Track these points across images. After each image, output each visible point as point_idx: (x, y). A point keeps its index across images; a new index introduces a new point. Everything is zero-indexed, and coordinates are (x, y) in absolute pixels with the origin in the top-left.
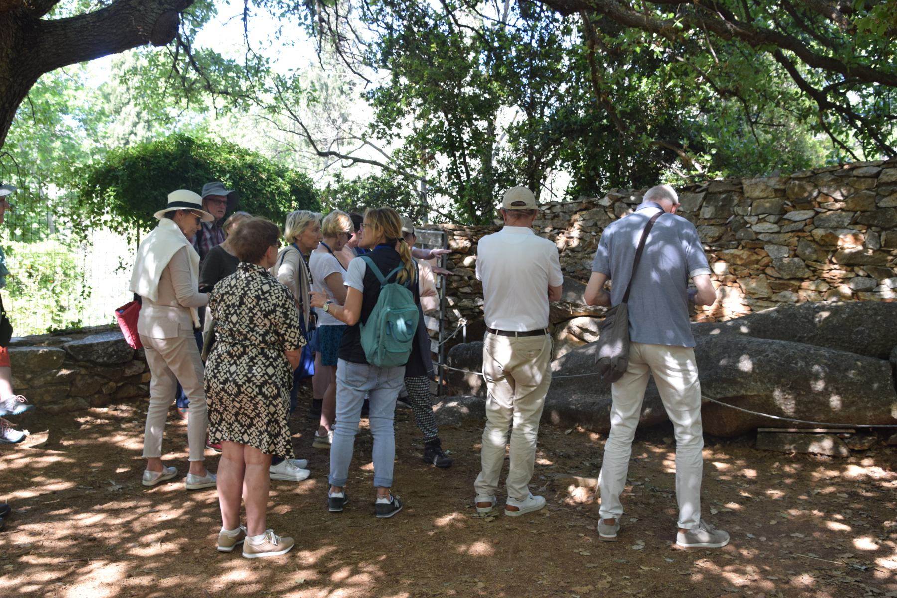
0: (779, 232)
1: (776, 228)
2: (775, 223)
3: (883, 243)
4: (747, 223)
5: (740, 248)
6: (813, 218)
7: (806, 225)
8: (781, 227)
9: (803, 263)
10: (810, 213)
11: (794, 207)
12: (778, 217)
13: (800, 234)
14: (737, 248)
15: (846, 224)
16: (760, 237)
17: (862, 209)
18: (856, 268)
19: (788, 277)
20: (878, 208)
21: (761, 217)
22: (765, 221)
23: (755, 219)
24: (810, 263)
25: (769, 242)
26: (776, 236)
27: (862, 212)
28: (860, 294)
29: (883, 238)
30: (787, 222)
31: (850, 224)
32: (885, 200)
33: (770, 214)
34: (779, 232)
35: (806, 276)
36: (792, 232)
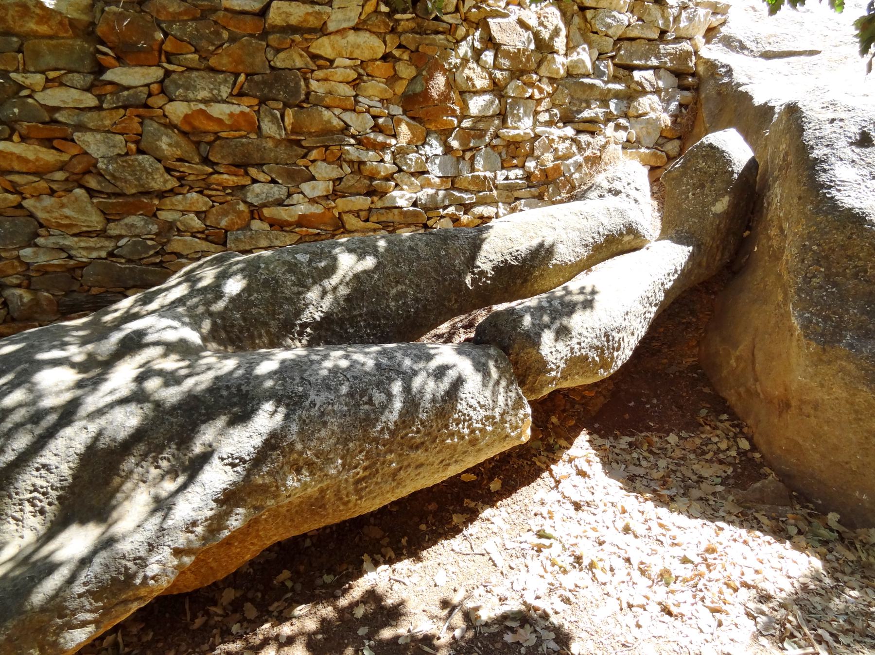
0: (99, 108)
1: (90, 100)
2: (88, 90)
3: (289, 128)
4: (22, 87)
5: (16, 138)
6: (161, 82)
7: (150, 95)
8: (100, 98)
9: (160, 166)
10: (155, 73)
11: (118, 59)
12: (90, 78)
13: (141, 111)
14: (9, 139)
15: (225, 95)
16: (58, 116)
17: (249, 71)
18: (253, 172)
19: (134, 191)
20: (273, 68)
21: (52, 75)
22: (62, 84)
23: (39, 78)
24: (171, 163)
25: (81, 127)
26: (95, 114)
27: (247, 75)
28: (266, 212)
29: (289, 119)
30: (109, 88)
31: (231, 94)
32: (282, 55)
33: (70, 71)
34: (99, 108)
35: (169, 186)
36: (125, 107)
